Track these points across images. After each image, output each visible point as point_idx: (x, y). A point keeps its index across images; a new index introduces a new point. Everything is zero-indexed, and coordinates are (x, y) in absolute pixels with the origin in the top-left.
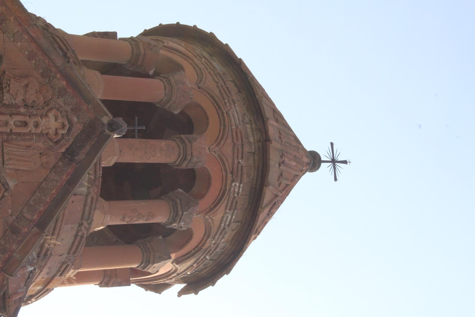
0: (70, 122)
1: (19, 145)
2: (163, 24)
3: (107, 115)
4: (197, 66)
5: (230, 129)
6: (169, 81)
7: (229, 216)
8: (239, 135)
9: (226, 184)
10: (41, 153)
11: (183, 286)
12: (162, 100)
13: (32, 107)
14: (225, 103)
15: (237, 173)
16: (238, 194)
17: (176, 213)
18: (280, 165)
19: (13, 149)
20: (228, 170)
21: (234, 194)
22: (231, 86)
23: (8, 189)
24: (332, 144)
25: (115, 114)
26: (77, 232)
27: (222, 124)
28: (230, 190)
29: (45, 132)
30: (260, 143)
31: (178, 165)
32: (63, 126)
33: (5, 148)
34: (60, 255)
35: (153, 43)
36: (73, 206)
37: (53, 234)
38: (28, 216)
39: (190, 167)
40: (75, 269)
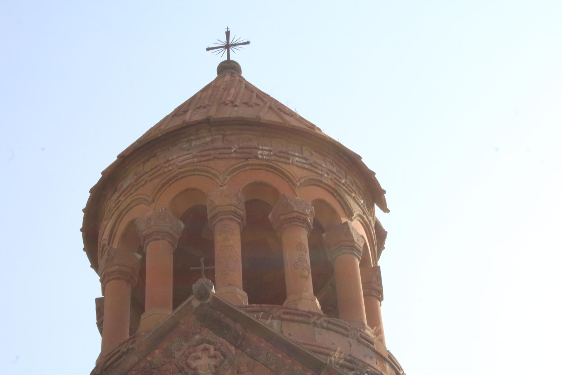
2: (83, 247)
3: (190, 302)
4: (129, 204)
5: (198, 164)
6: (147, 236)
9: (260, 165)
10: (238, 373)
11: (377, 208)
12: (169, 242)
14: (169, 171)
15: (247, 153)
16: (270, 151)
18: (236, 106)
20: (245, 163)
22: (148, 166)
24: (208, 49)
25: (189, 293)
26: (323, 328)
27: (193, 173)
28: (266, 160)
29: (213, 369)
31: (242, 220)
32: (205, 349)
34: (350, 346)
35: (105, 257)
36: (294, 333)
37: (328, 355)
39: (242, 206)
40: (364, 327)
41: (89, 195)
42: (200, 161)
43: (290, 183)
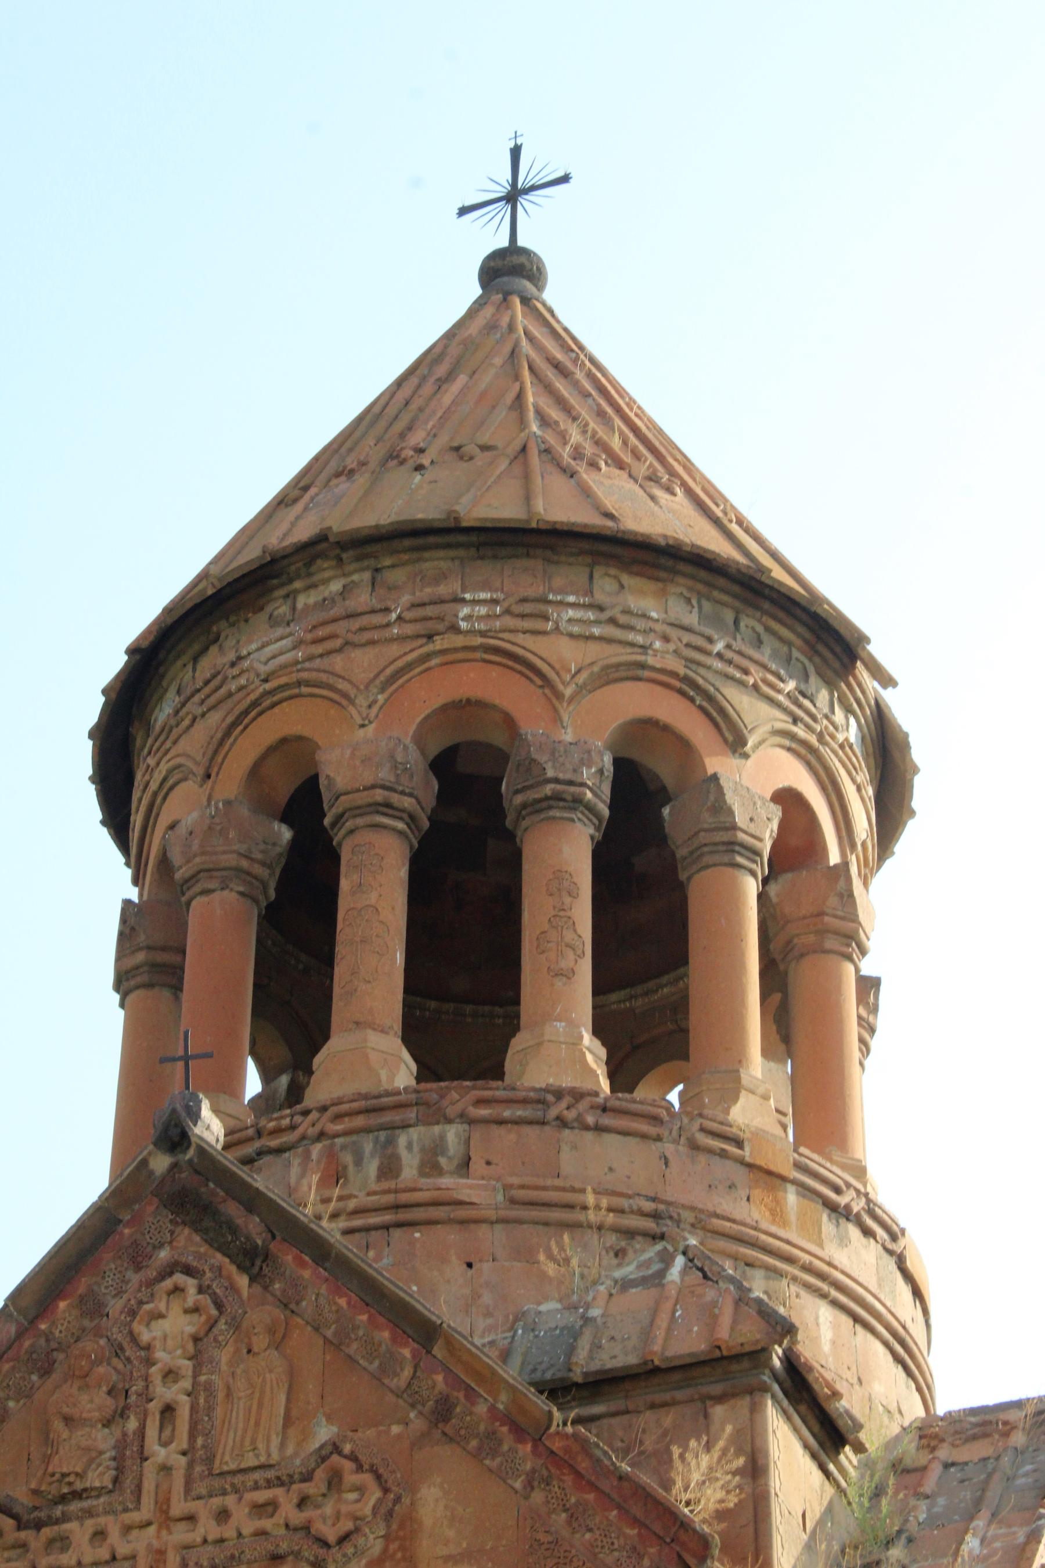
0: (169, 1270)
1: (224, 1422)
4: (165, 780)
5: (307, 665)
6: (187, 881)
7: (565, 617)
8: (320, 633)
9: (465, 648)
10: (249, 1351)
12: (241, 894)
13: (127, 1392)
14: (241, 688)
16: (495, 602)
17: (552, 802)
19: (230, 1442)
21: (498, 617)
23: (334, 1444)
24: (463, 211)
26: (587, 1128)
27: (296, 691)
28: (483, 634)
29: (190, 1348)
30: (344, 556)
31: (412, 819)
32: (177, 1290)
33: (225, 1468)
34: (666, 1164)
38: (407, 1373)
41: (90, 744)
42: (311, 658)
43: (547, 691)
